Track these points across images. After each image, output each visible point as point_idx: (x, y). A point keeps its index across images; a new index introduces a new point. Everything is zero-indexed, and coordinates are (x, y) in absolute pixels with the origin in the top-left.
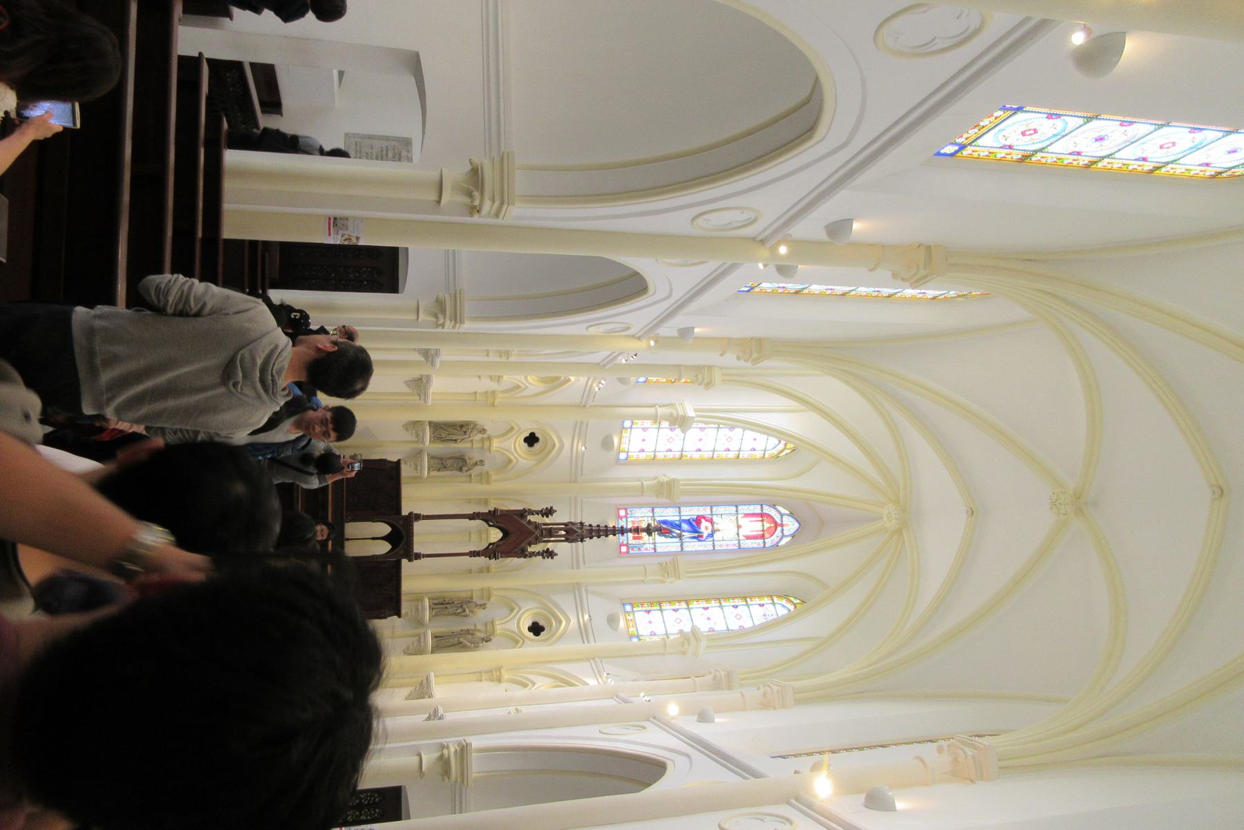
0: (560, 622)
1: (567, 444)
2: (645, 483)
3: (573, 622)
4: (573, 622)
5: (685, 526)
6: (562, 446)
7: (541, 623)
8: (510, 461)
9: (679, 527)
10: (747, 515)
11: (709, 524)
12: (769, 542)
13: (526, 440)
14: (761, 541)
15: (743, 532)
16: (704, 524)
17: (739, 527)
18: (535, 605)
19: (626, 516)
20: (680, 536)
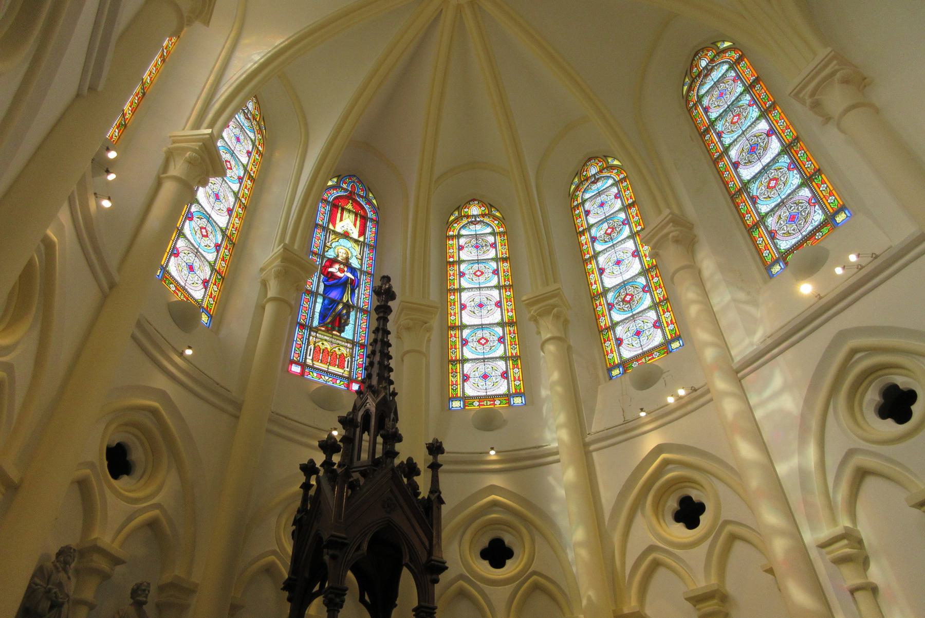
0: (495, 504)
1: (161, 382)
2: (271, 294)
3: (496, 480)
4: (496, 480)
5: (334, 294)
6: (163, 396)
7: (485, 542)
8: (152, 525)
9: (334, 302)
10: (332, 220)
11: (337, 266)
12: (370, 215)
13: (115, 474)
14: (369, 224)
15: (355, 234)
16: (334, 269)
17: (346, 235)
18: (456, 544)
19: (304, 365)
20: (348, 306)
